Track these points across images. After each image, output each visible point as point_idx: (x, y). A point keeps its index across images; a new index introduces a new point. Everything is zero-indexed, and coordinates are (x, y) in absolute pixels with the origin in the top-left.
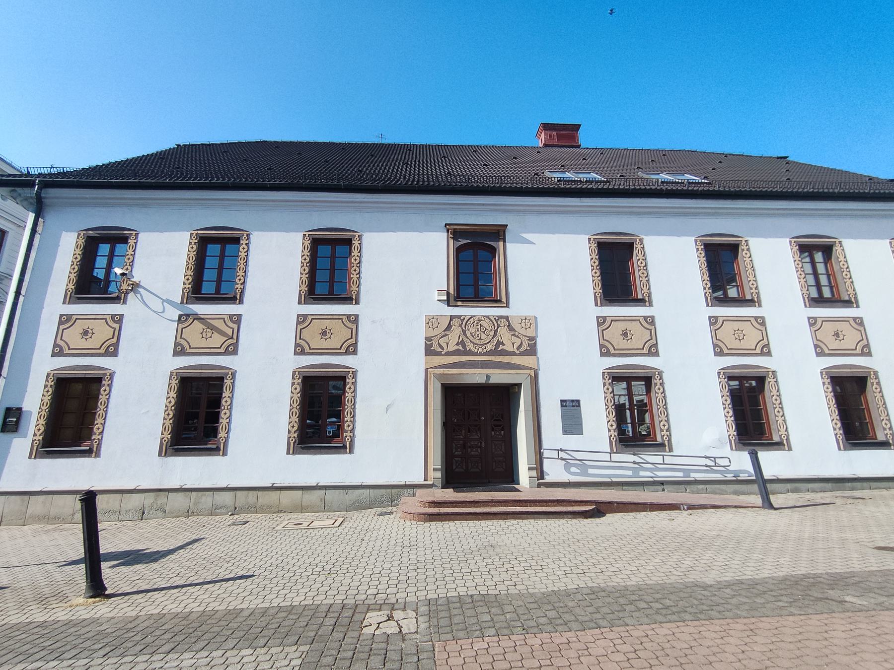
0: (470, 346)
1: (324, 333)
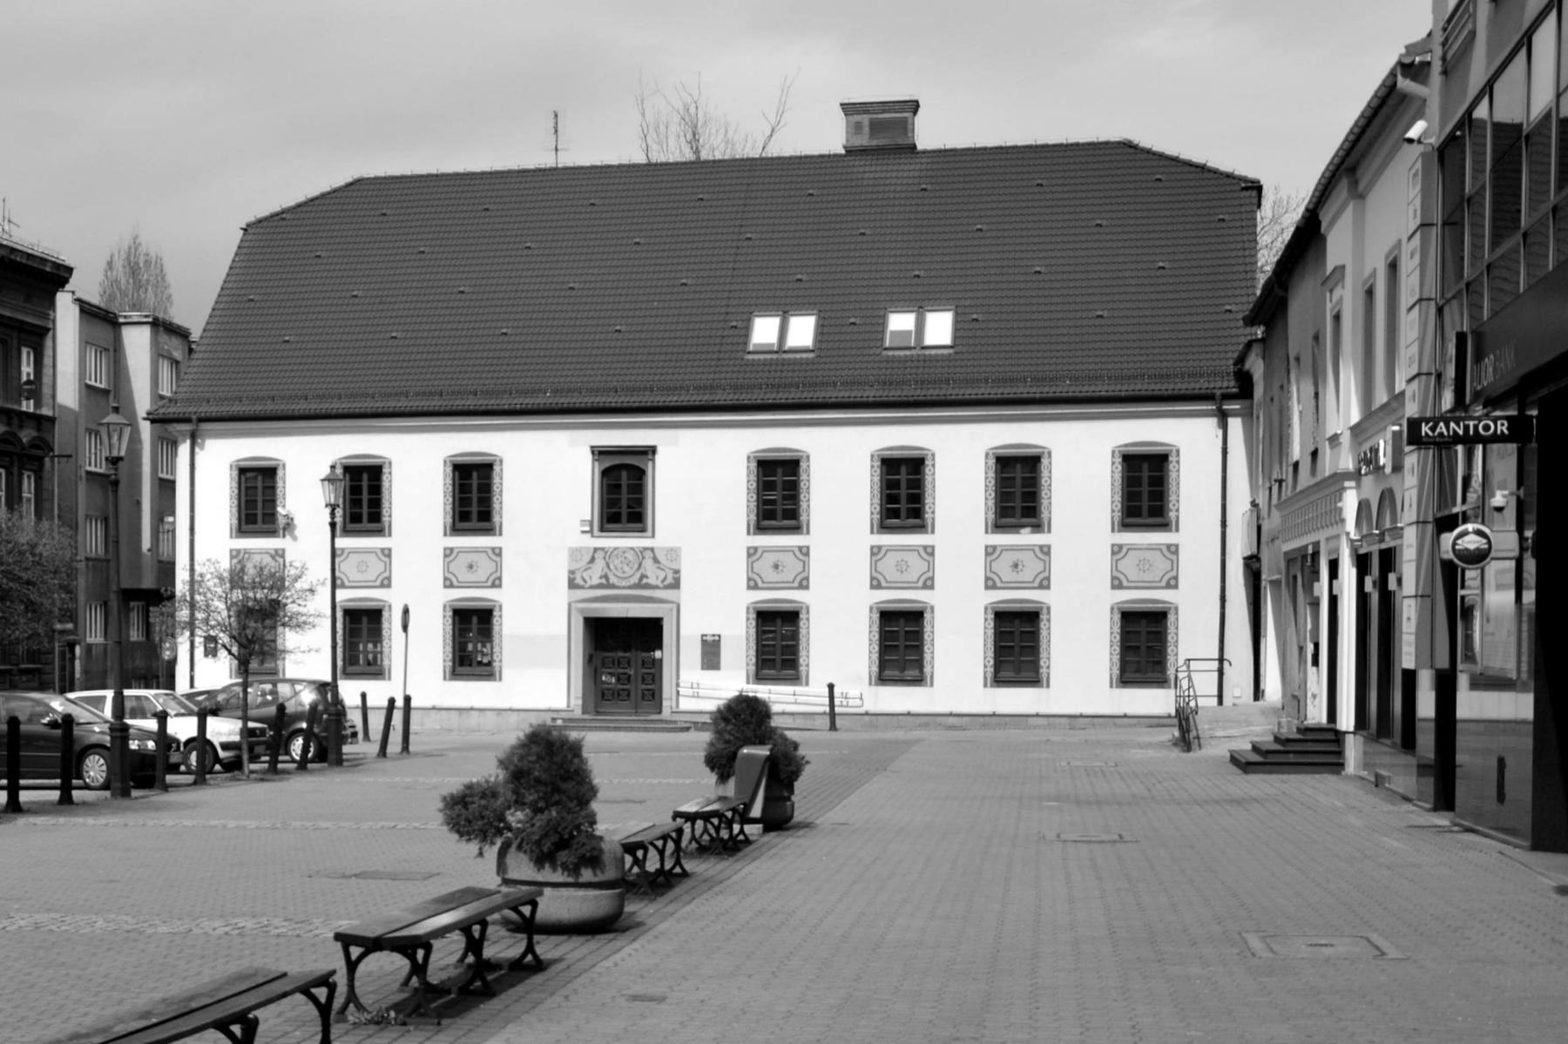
0: (613, 580)
1: (471, 567)
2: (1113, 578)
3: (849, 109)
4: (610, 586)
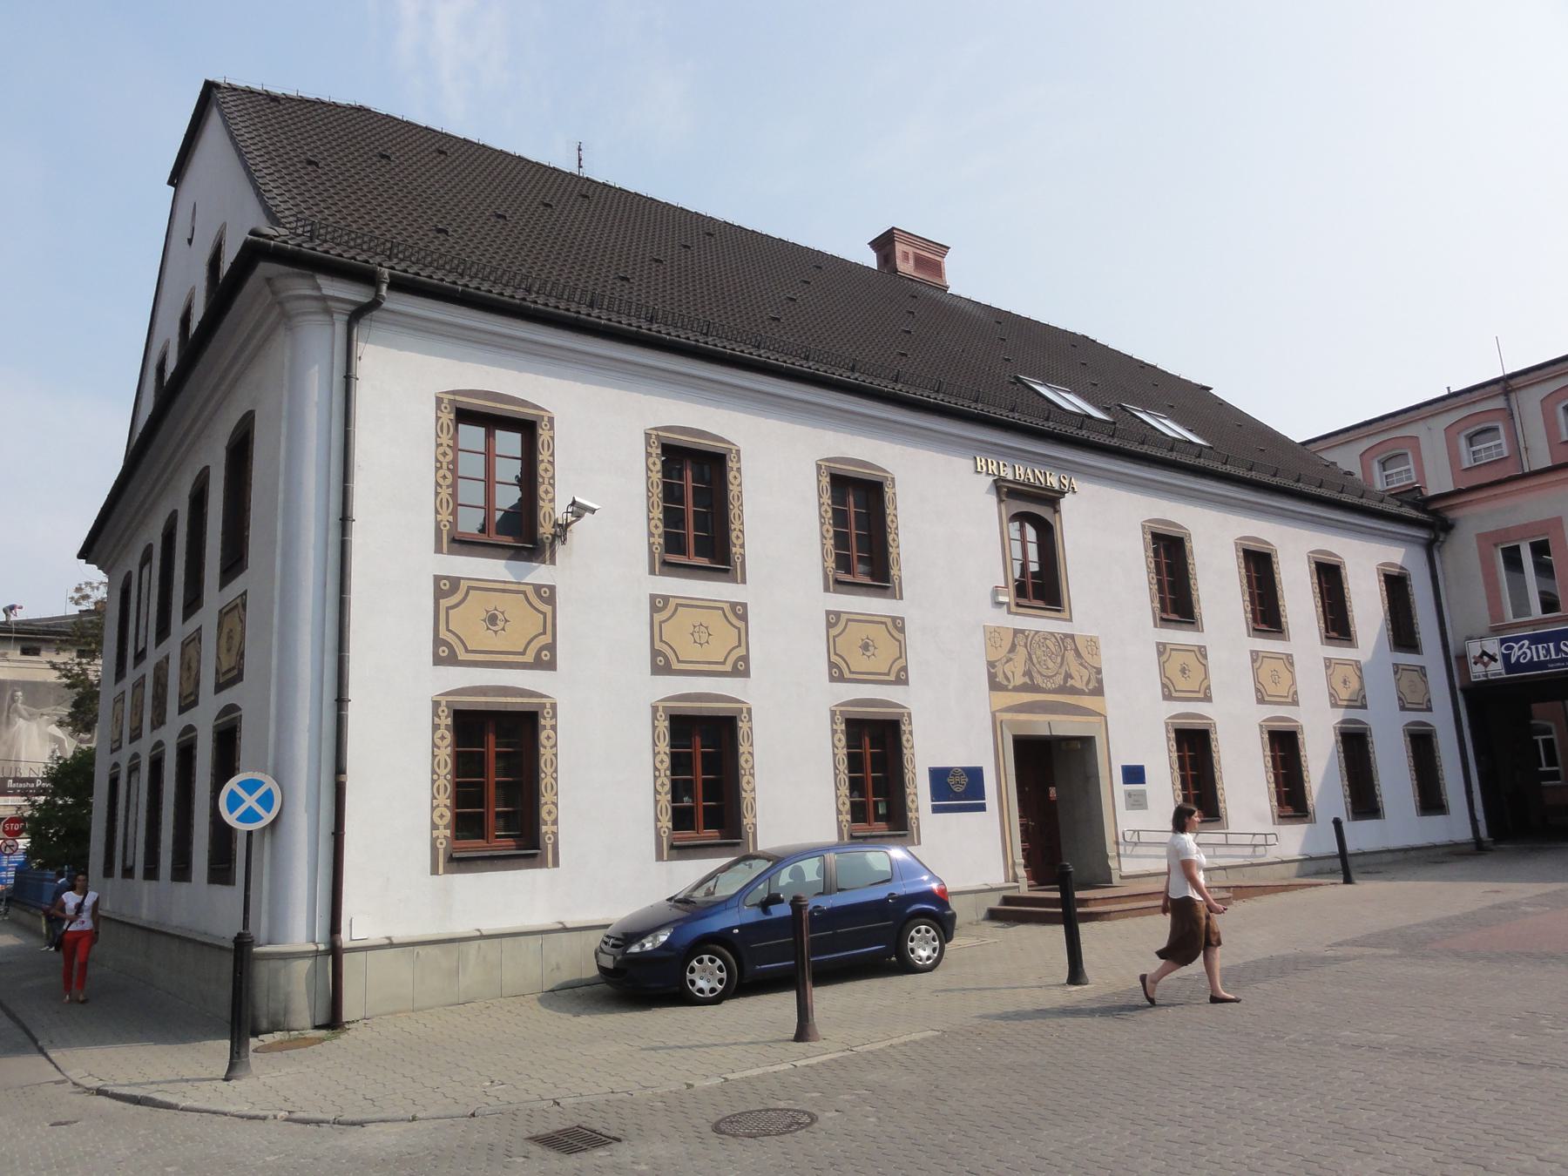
0: (1039, 680)
4: (1034, 688)
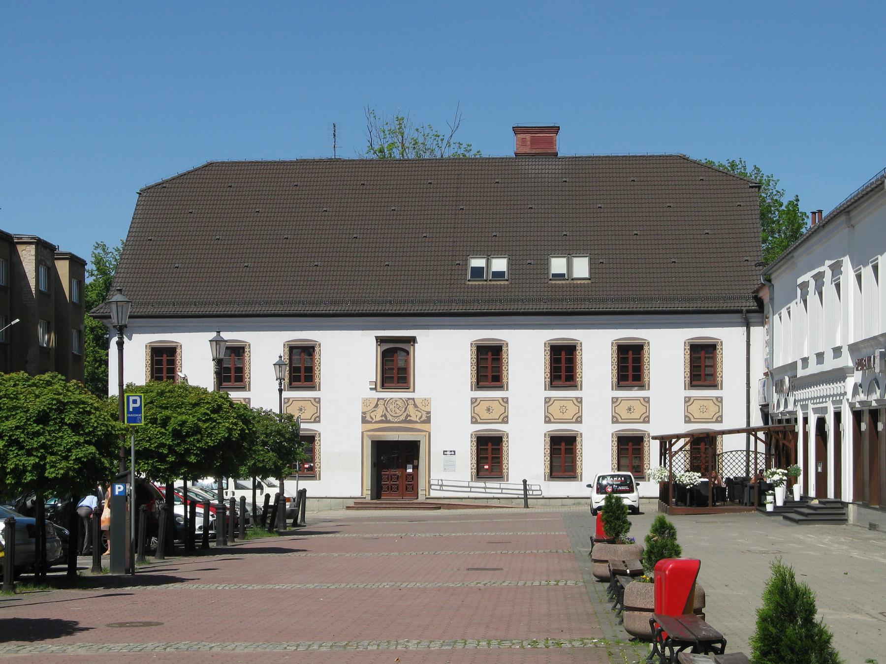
0: (390, 418)
2: (686, 417)
3: (517, 130)
